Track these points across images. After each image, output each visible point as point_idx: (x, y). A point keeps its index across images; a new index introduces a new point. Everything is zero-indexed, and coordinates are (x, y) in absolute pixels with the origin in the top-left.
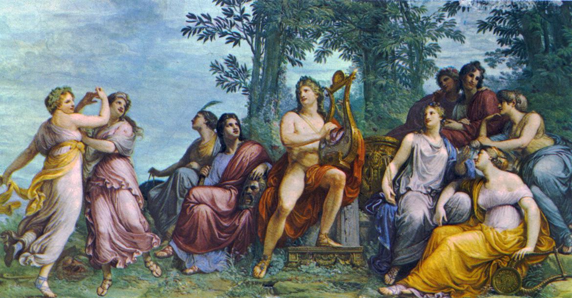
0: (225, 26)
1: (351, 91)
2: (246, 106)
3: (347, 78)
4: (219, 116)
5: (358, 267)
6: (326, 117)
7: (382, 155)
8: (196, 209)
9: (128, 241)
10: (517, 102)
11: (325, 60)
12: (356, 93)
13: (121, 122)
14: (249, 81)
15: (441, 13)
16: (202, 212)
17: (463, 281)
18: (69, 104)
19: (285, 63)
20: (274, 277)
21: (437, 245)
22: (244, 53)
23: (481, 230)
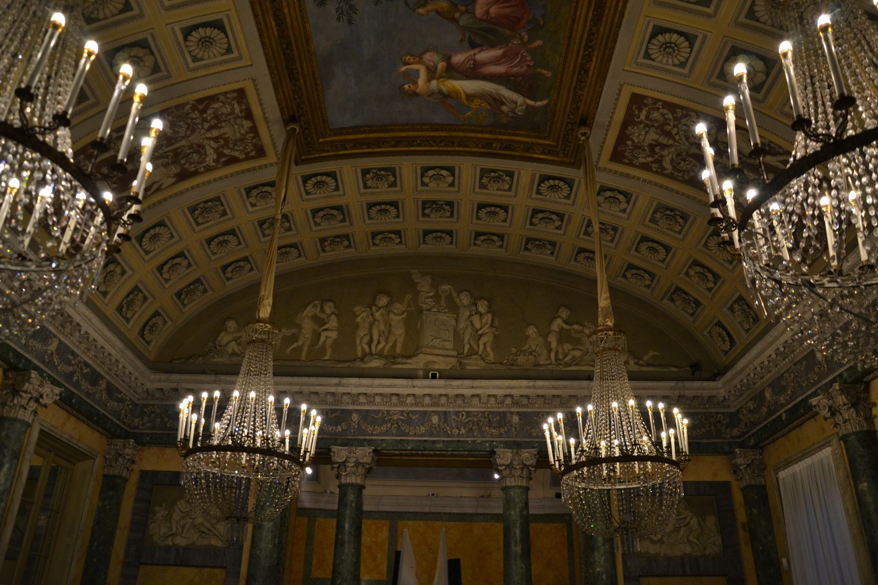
8: (492, 15)
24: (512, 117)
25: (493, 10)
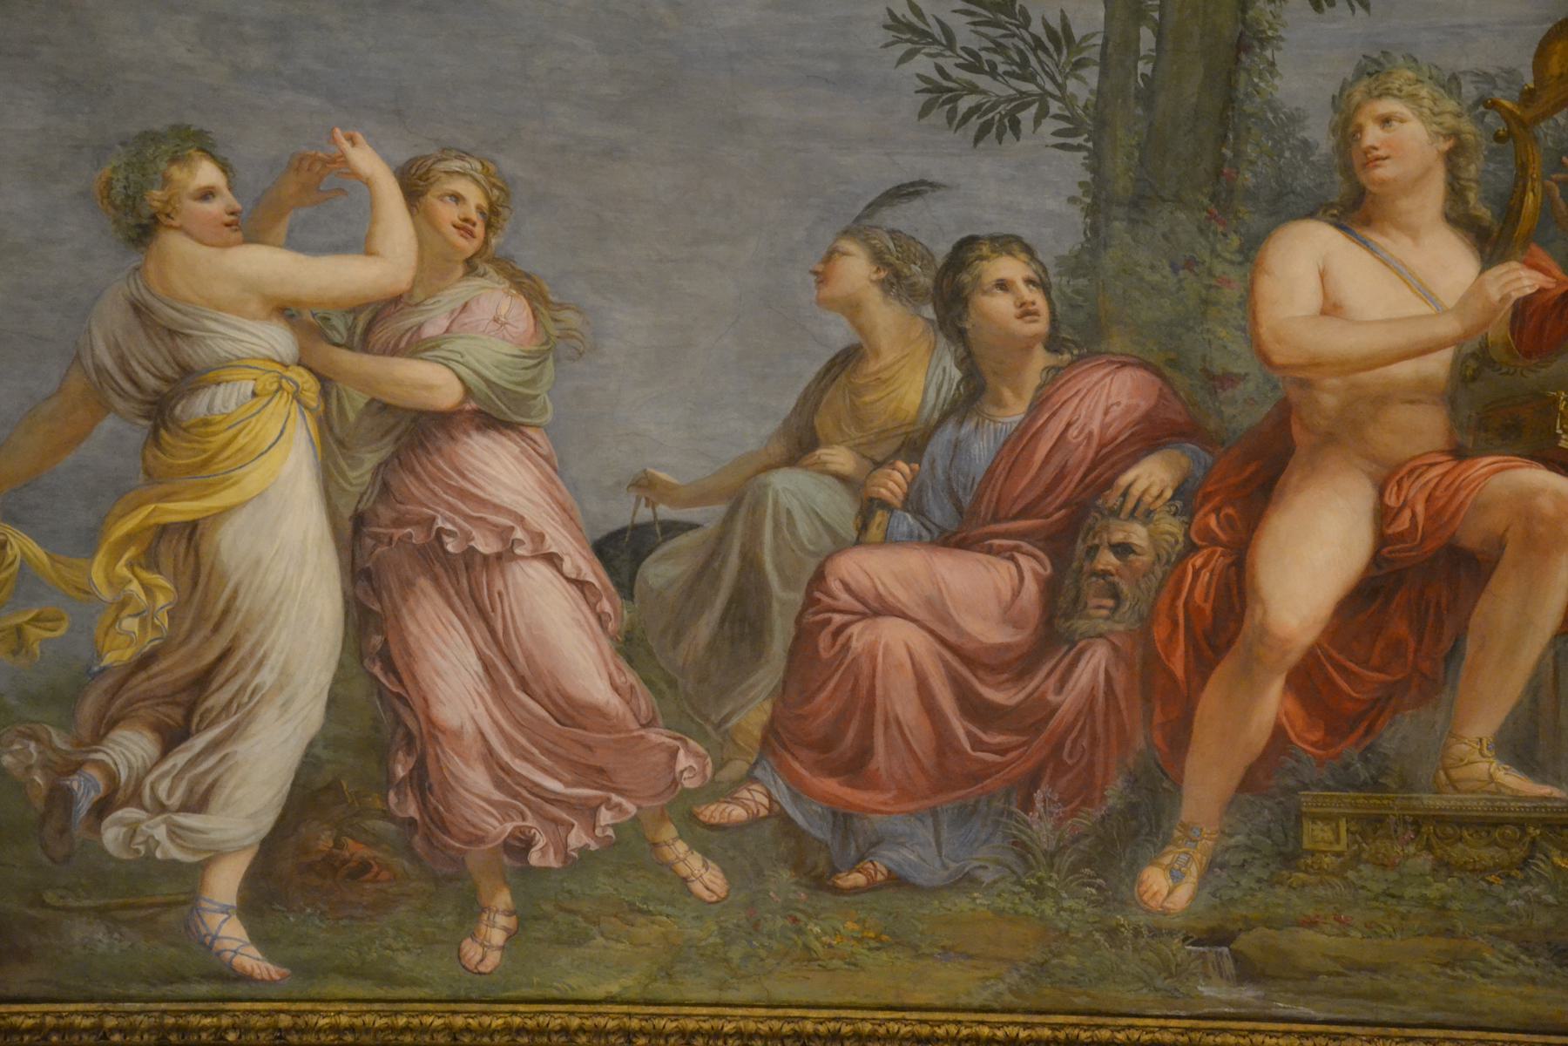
2: (1072, 200)
4: (942, 250)
6: (1490, 241)
8: (860, 636)
9: (573, 765)
13: (477, 282)
14: (1083, 87)
16: (886, 646)
18: (215, 208)
20: (1241, 910)
24: (61, 798)
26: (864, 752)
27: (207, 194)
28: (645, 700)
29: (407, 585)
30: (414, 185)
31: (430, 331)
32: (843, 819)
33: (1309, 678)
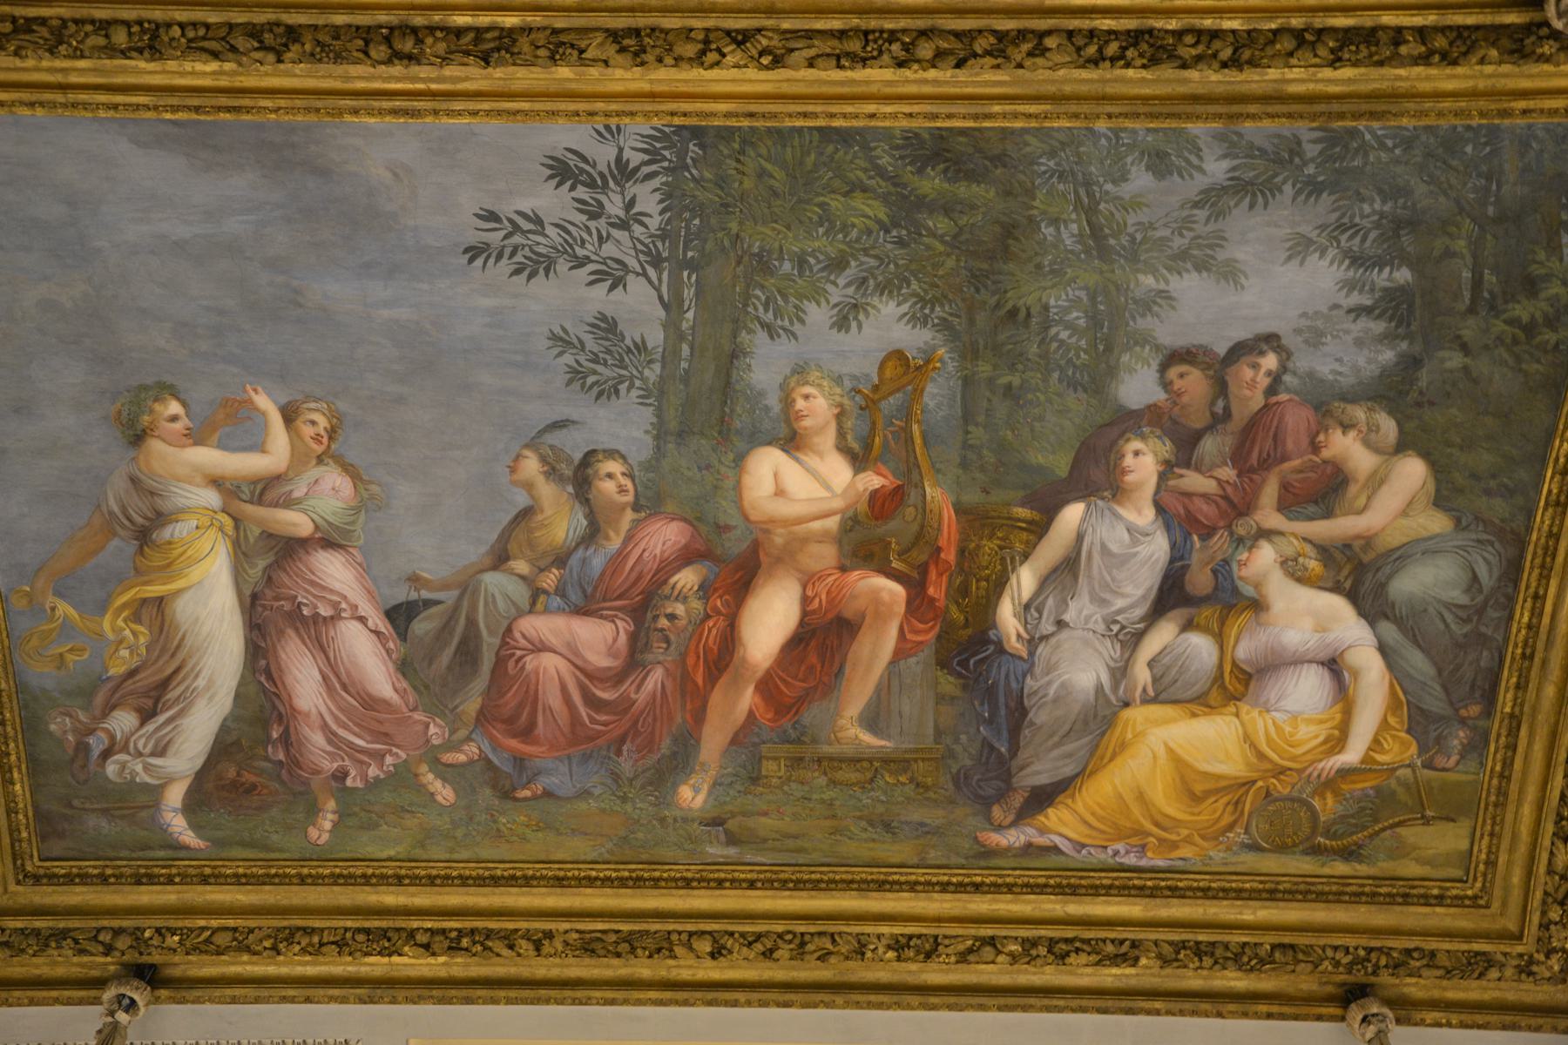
0: (583, 242)
1: (926, 399)
2: (647, 432)
3: (918, 368)
4: (578, 456)
5: (927, 788)
6: (859, 460)
7: (1001, 548)
8: (530, 662)
9: (372, 732)
10: (1370, 430)
11: (860, 327)
12: (939, 406)
13: (323, 468)
14: (653, 373)
15: (1185, 213)
17: (1174, 819)
18: (178, 426)
19: (751, 331)
20: (730, 807)
21: (1123, 746)
22: (639, 306)
23: (1237, 715)
24: (83, 748)
25: (550, 665)
26: (532, 725)
27: (174, 418)
28: (412, 697)
29: (281, 633)
30: (290, 415)
31: (296, 494)
32: (519, 761)
33: (767, 686)
